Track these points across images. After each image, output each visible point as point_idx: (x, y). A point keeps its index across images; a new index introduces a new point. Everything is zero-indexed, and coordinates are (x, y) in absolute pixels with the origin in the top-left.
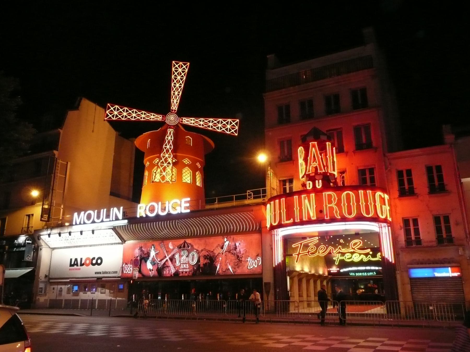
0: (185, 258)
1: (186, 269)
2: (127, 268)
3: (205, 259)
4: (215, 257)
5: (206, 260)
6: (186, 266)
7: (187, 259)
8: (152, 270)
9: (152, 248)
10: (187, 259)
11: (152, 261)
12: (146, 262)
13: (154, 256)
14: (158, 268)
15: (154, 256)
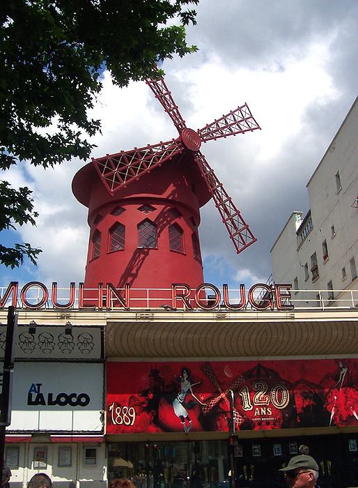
0: (262, 396)
1: (268, 417)
2: (121, 415)
3: (305, 398)
4: (324, 395)
5: (308, 400)
6: (267, 411)
7: (267, 399)
8: (188, 418)
9: (183, 375)
10: (267, 399)
11: (187, 402)
12: (171, 402)
13: (189, 390)
14: (201, 414)
15: (189, 390)
